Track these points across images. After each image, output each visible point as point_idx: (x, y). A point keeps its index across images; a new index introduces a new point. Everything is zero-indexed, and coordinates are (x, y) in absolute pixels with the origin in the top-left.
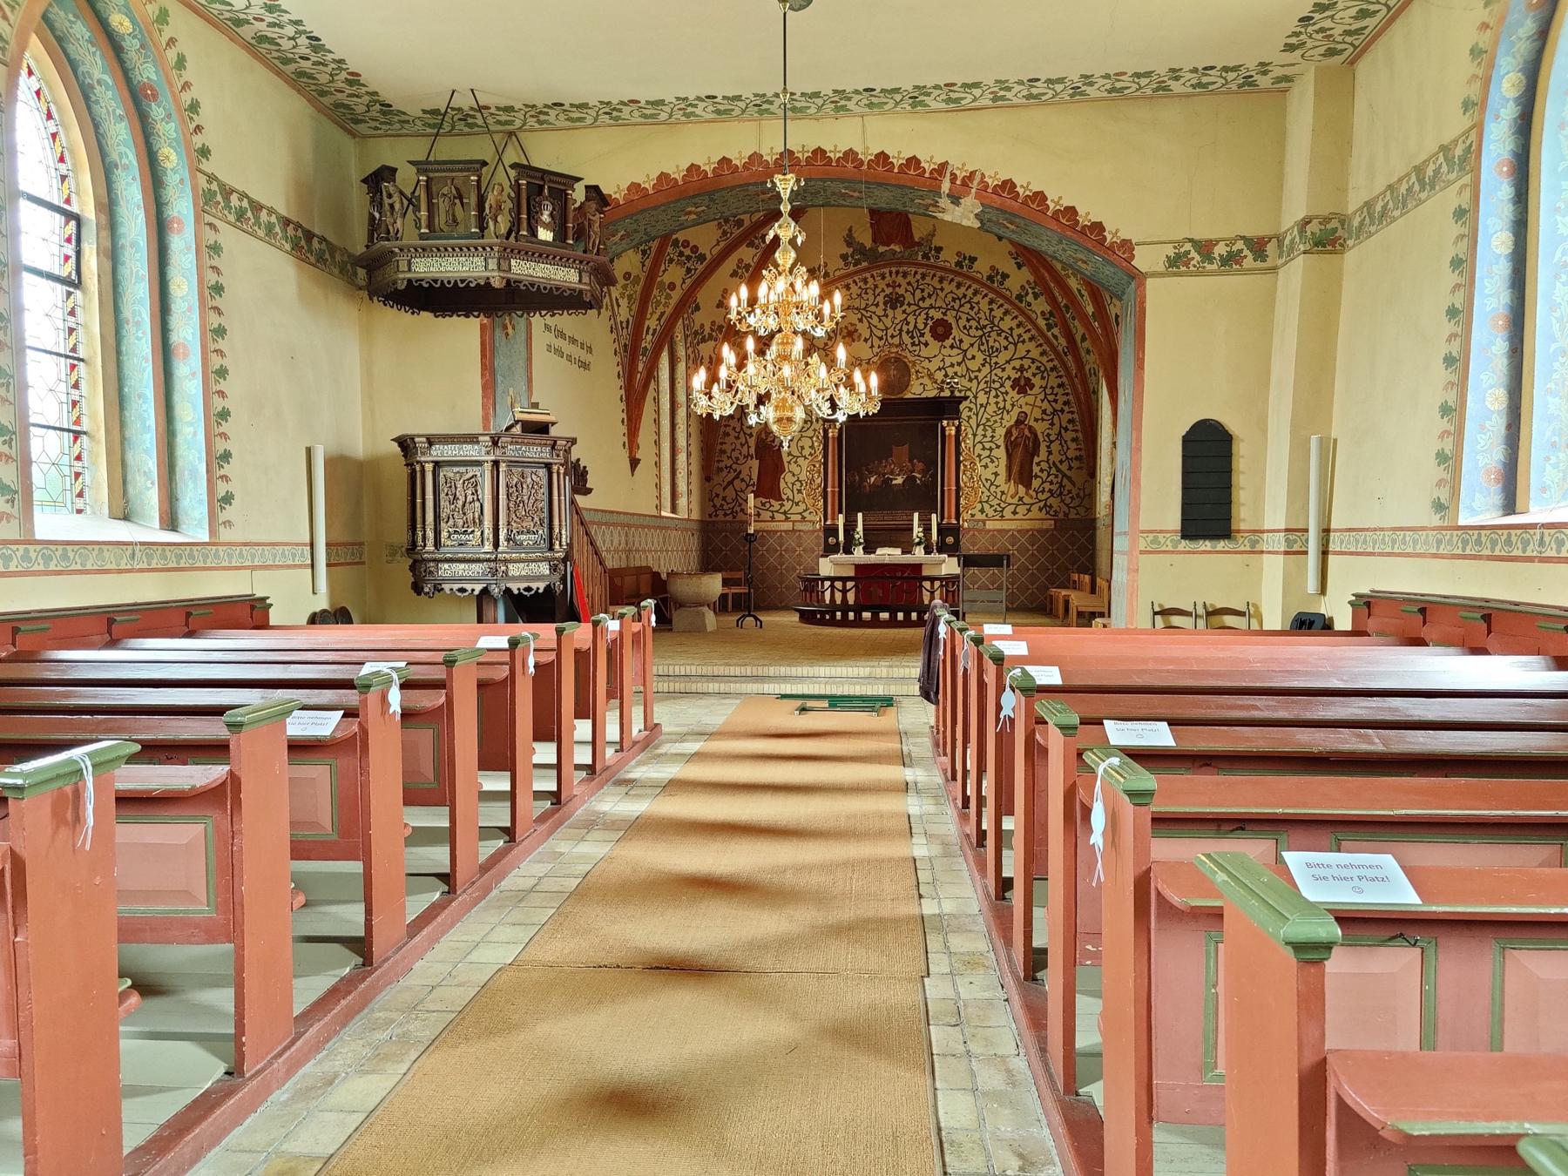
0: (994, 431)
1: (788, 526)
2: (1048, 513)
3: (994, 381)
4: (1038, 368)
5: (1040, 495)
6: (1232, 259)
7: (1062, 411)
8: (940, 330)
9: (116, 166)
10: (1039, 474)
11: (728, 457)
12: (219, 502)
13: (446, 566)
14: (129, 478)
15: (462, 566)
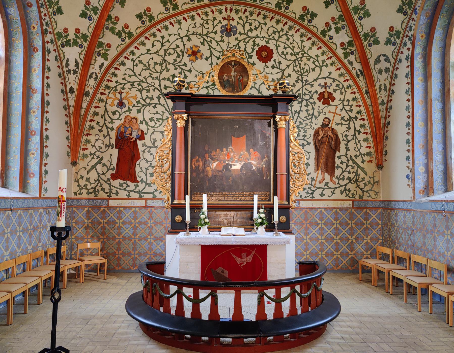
0: (305, 131)
1: (141, 203)
2: (347, 195)
3: (305, 94)
4: (337, 86)
5: (341, 181)
7: (356, 118)
8: (264, 54)
10: (340, 165)
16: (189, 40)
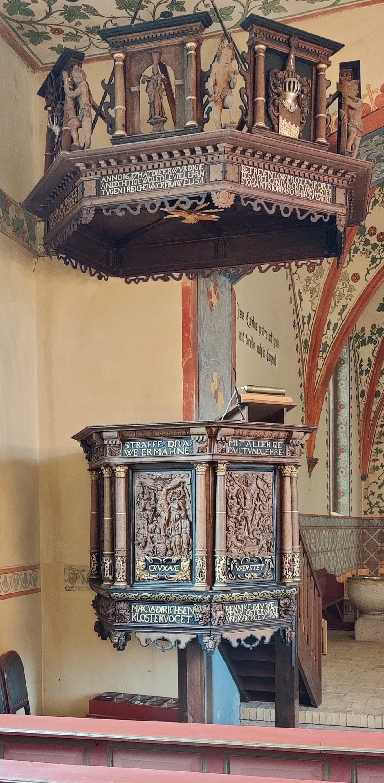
13: (142, 608)
15: (163, 609)
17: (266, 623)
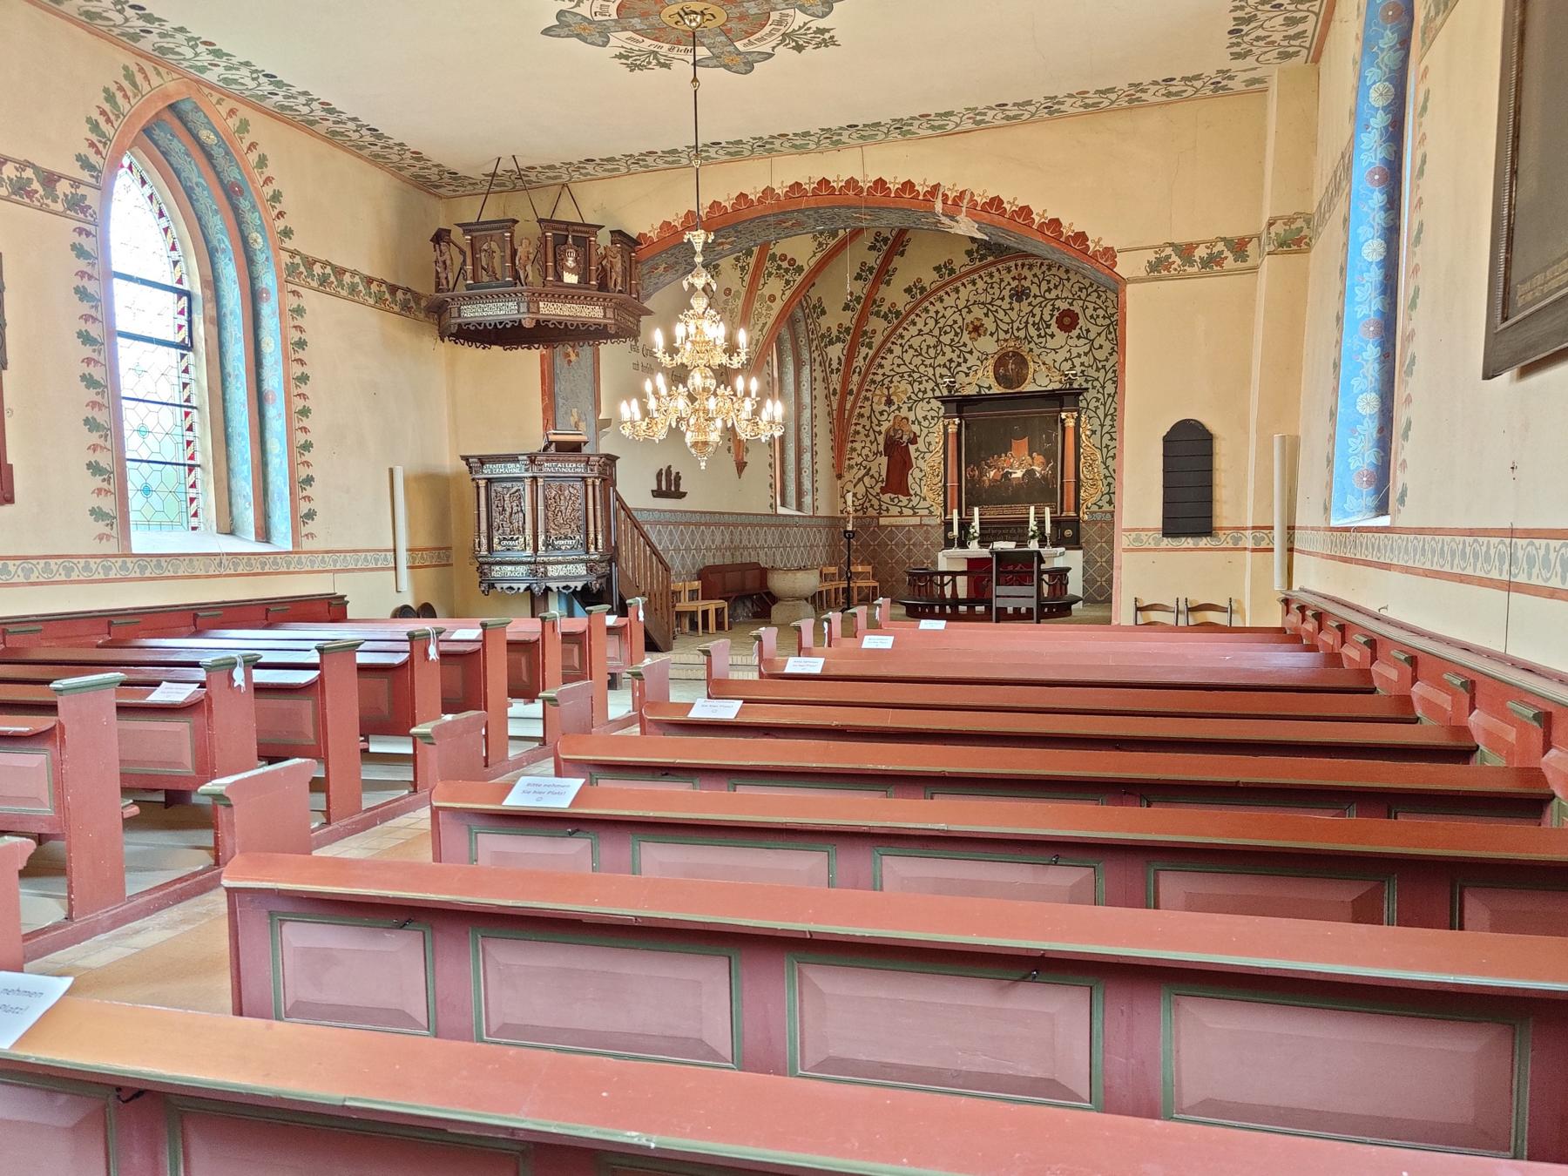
1: (916, 521)
6: (1213, 261)
8: (1067, 320)
9: (217, 250)
11: (859, 455)
12: (304, 517)
13: (497, 568)
14: (233, 501)
15: (510, 568)
16: (970, 312)
17: (575, 578)
